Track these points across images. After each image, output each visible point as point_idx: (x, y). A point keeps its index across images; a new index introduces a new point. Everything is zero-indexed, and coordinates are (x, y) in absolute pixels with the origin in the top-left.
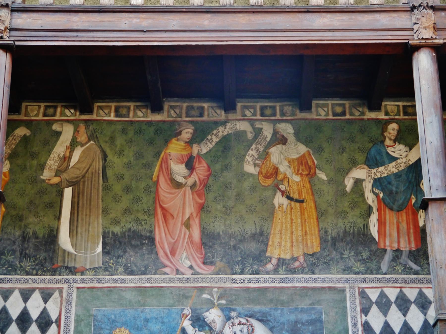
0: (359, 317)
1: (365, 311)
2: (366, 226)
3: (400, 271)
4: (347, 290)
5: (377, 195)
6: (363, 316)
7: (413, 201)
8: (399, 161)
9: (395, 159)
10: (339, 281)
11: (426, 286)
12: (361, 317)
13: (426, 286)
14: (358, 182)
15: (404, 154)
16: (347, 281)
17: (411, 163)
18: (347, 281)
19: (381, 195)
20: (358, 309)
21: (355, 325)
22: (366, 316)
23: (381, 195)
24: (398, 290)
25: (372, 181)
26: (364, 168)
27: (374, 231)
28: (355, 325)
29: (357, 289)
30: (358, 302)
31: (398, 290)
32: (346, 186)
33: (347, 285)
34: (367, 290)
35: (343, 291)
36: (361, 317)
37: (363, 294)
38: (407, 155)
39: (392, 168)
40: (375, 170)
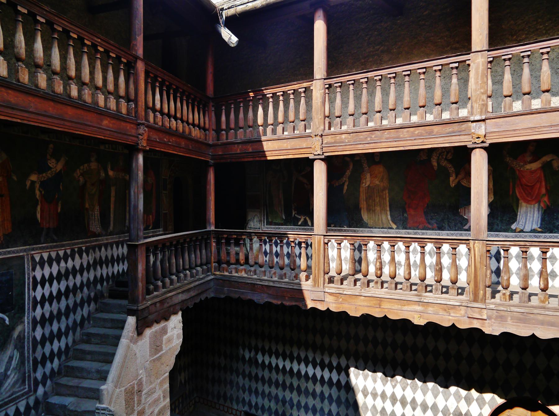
0: (31, 273)
1: (34, 269)
2: (35, 213)
3: (49, 241)
4: (26, 257)
5: (41, 192)
6: (33, 272)
7: (57, 196)
8: (52, 170)
9: (51, 168)
10: (21, 251)
11: (60, 249)
12: (32, 273)
13: (60, 249)
14: (33, 183)
15: (55, 165)
16: (25, 250)
17: (57, 171)
18: (25, 250)
19: (43, 192)
20: (31, 268)
21: (29, 279)
22: (34, 272)
23: (43, 192)
24: (48, 253)
25: (39, 183)
26: (36, 174)
27: (39, 216)
28: (29, 279)
29: (30, 256)
30: (30, 264)
31: (48, 253)
32: (26, 185)
33: (25, 254)
34: (34, 255)
35: (22, 258)
36: (32, 273)
37: (33, 259)
38: (56, 166)
39: (49, 174)
40: (41, 176)
